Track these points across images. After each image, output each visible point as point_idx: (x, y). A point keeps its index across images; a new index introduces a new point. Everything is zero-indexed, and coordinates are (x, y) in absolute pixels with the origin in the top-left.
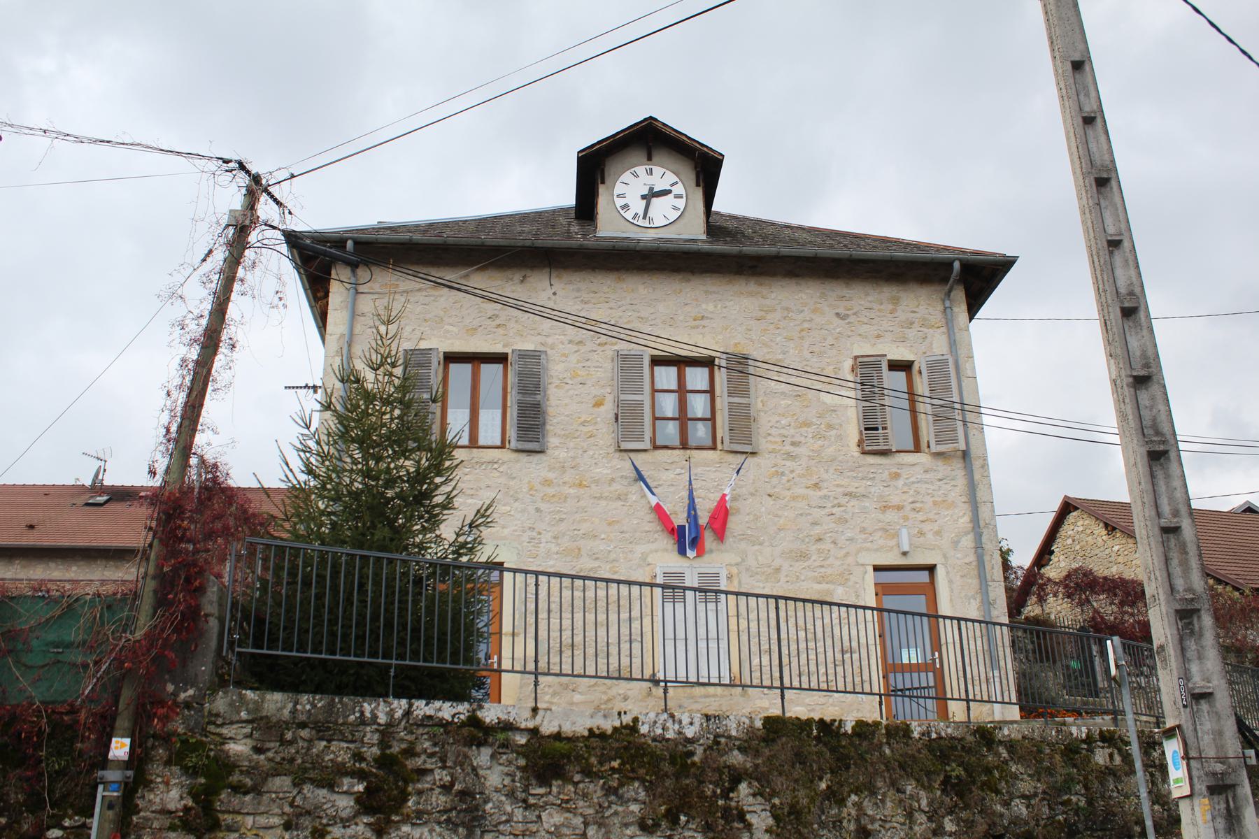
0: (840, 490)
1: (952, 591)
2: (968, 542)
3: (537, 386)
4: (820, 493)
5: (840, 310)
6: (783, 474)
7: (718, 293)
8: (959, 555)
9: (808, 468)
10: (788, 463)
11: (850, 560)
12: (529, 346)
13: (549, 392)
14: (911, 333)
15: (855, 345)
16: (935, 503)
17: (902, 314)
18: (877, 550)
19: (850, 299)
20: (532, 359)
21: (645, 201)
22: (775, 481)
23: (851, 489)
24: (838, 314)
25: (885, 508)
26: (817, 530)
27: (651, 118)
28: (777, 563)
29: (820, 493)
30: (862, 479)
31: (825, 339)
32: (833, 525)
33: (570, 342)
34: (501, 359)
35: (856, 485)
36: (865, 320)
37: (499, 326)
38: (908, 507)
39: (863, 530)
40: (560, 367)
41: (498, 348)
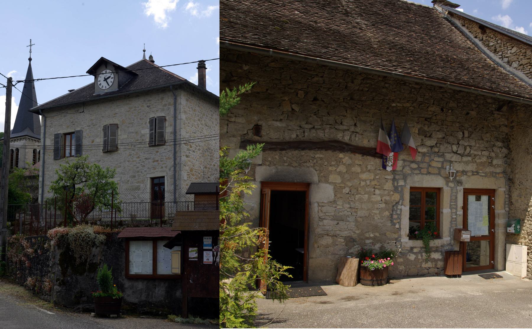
0: (144, 158)
1: (168, 183)
2: (172, 169)
3: (80, 139)
4: (139, 159)
5: (148, 105)
6: (131, 155)
7: (119, 106)
8: (171, 173)
9: (137, 153)
10: (133, 152)
11: (145, 177)
12: (79, 129)
13: (83, 141)
14: (165, 108)
15: (151, 115)
16: (166, 158)
17: (164, 103)
18: (151, 173)
19: (151, 101)
20: (78, 132)
21: (105, 81)
22: (129, 157)
23: (147, 157)
24: (147, 106)
25: (154, 162)
26: (138, 169)
27: (102, 57)
28: (129, 179)
29: (139, 159)
30: (150, 154)
31: (144, 114)
32: (142, 168)
33: (87, 126)
34: (73, 133)
35: (148, 156)
36: (154, 106)
37: (73, 124)
38: (159, 161)
39: (149, 168)
40: (85, 134)
41: (73, 131)
